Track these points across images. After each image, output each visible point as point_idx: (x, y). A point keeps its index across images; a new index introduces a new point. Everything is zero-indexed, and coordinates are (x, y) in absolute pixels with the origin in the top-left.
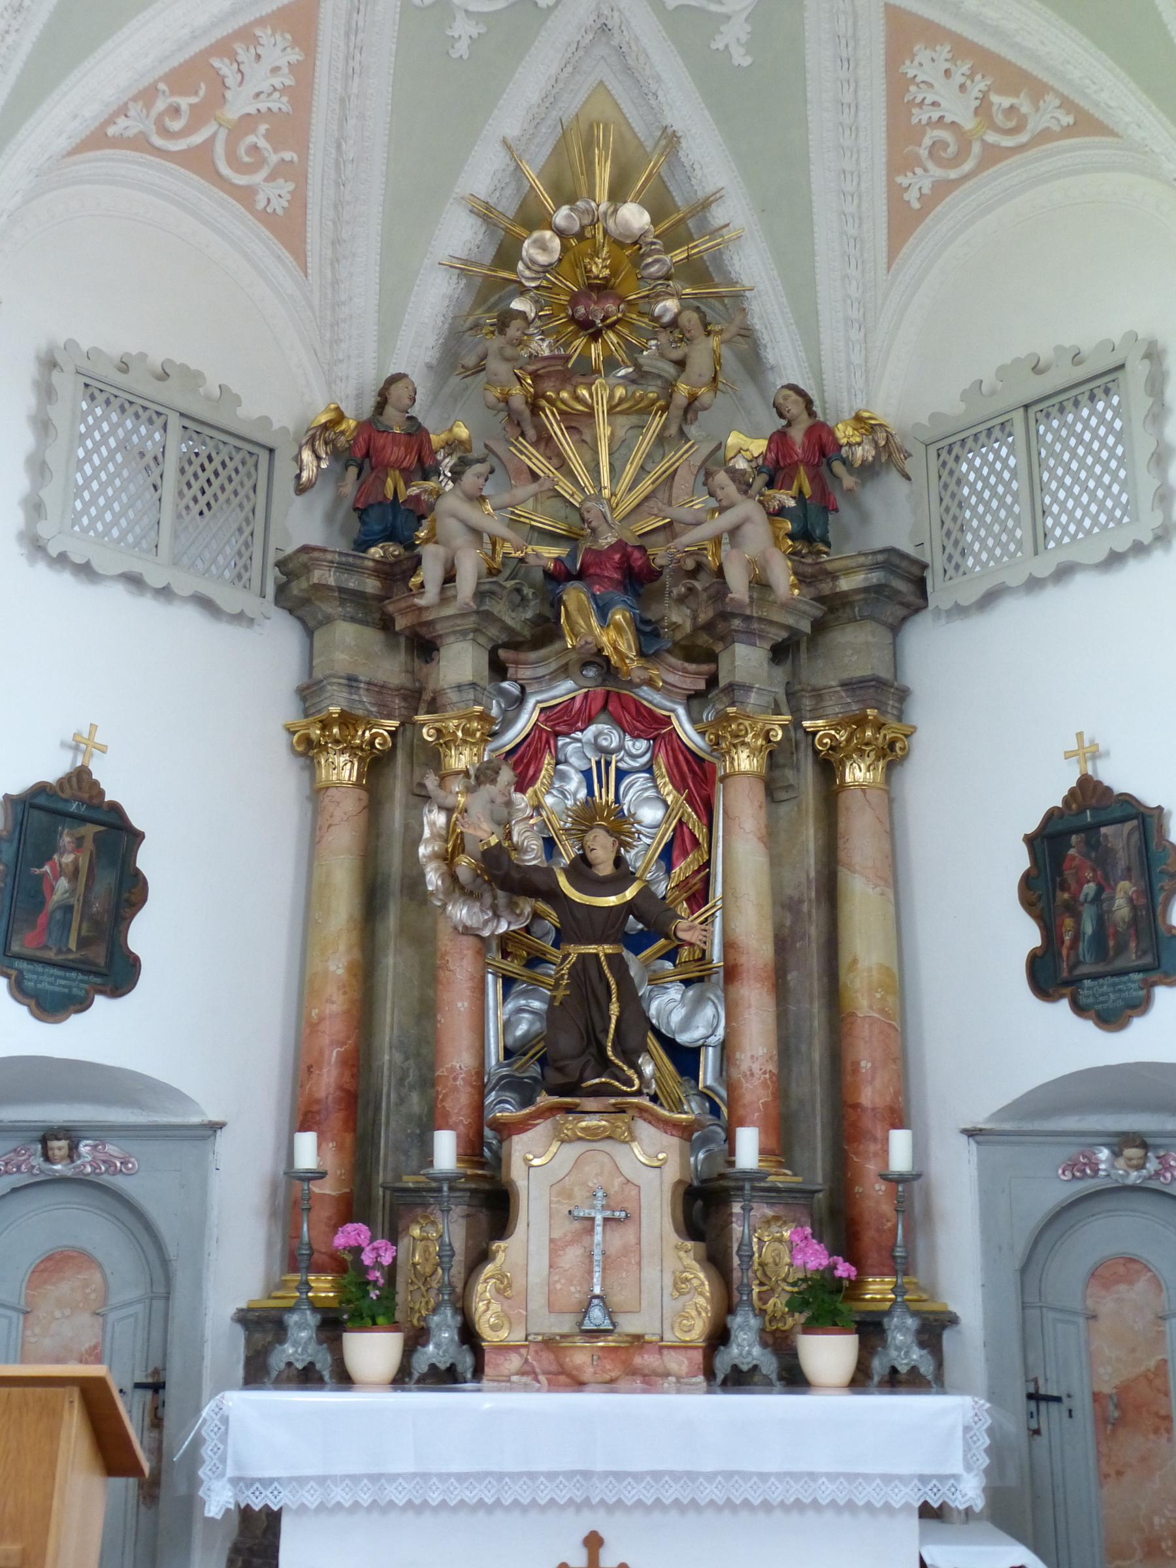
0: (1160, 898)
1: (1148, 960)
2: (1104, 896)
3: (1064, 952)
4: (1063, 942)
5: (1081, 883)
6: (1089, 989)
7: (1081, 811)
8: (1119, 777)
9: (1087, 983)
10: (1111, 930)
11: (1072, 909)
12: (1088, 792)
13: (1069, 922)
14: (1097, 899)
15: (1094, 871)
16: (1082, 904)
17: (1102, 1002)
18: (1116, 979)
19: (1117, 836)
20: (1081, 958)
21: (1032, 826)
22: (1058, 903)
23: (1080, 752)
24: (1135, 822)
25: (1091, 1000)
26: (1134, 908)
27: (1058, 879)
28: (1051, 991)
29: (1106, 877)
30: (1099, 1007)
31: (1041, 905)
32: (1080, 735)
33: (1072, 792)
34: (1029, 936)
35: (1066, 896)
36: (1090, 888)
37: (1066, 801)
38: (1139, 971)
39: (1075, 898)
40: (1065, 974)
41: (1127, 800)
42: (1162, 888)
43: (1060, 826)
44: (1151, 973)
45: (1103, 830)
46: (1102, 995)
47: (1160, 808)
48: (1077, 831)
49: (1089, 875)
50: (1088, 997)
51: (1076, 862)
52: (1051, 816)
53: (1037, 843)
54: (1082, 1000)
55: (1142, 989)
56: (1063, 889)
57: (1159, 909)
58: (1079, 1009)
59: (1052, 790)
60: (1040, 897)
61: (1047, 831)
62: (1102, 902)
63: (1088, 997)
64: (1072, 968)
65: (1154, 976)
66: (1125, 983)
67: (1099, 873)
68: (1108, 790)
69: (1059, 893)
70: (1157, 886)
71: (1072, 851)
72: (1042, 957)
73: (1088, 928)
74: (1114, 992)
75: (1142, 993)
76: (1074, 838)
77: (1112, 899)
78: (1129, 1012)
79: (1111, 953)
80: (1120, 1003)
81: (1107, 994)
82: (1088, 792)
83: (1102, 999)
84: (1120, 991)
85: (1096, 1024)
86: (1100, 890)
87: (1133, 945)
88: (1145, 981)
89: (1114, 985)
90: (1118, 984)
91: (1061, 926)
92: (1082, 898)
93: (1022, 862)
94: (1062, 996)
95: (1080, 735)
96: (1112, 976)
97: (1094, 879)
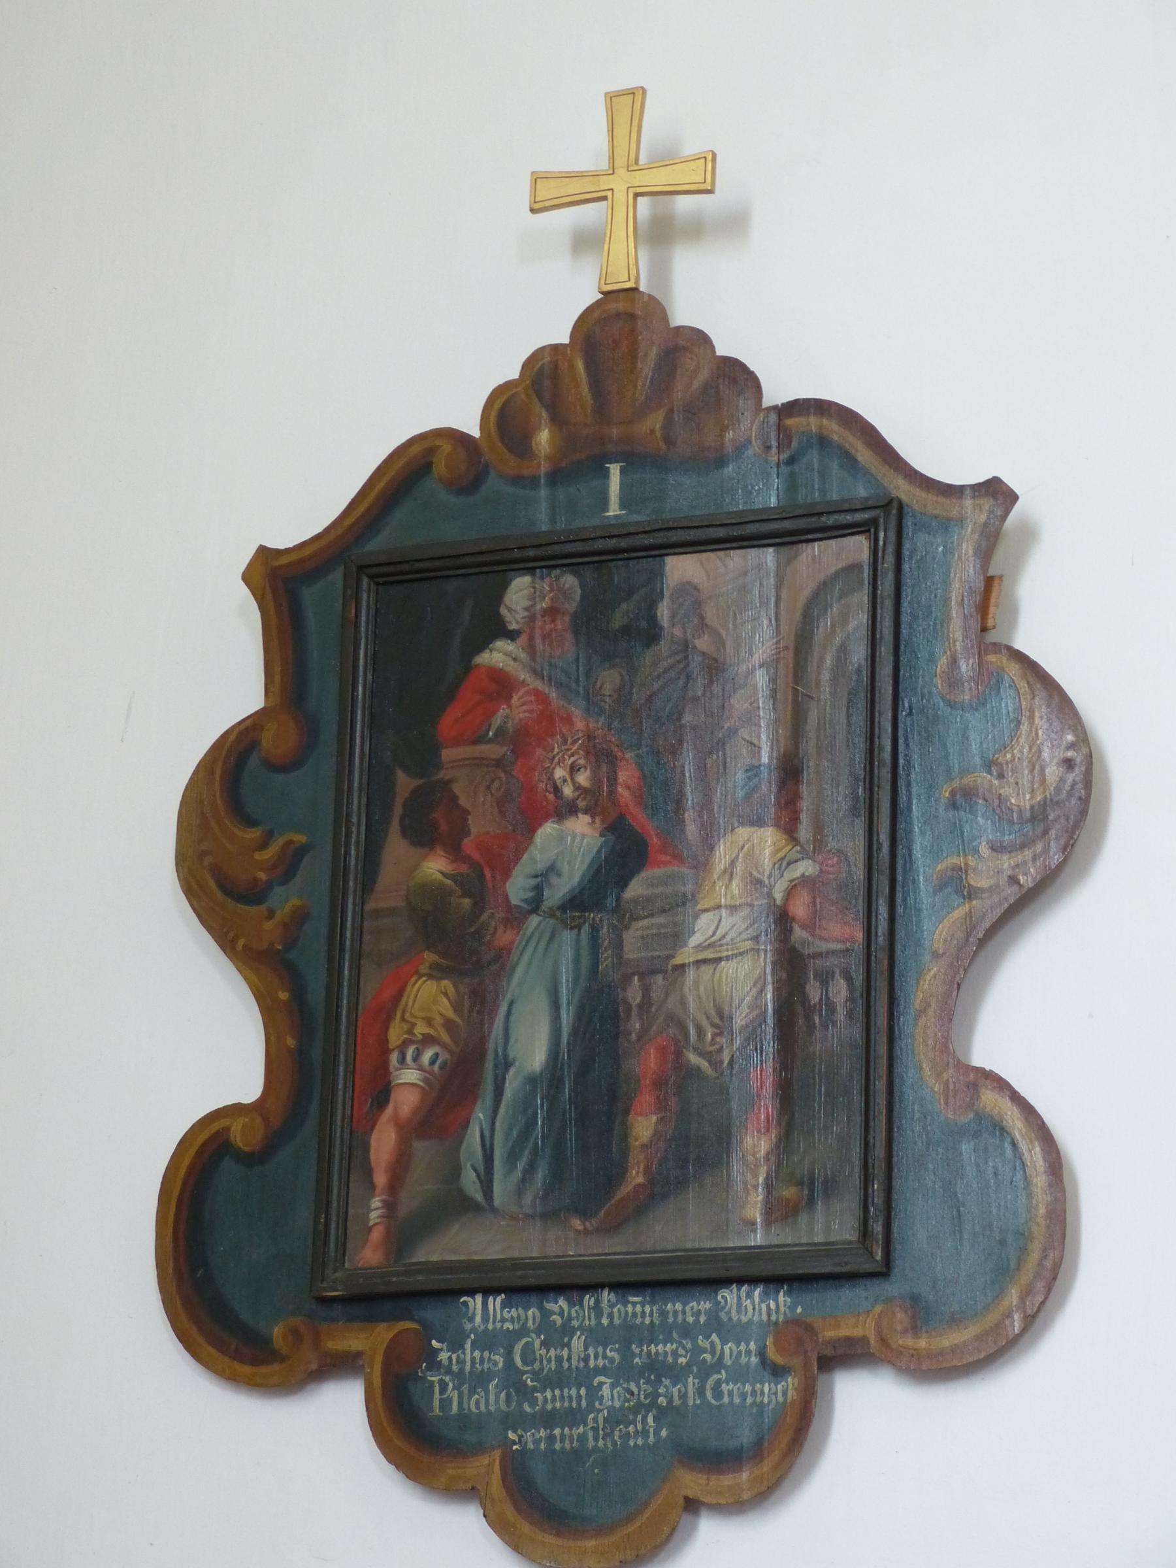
0: (937, 927)
1: (833, 1225)
2: (636, 889)
3: (383, 1143)
4: (382, 1094)
5: (534, 809)
6: (487, 1342)
7: (580, 465)
8: (783, 318)
9: (484, 1312)
10: (647, 1062)
11: (462, 940)
12: (624, 380)
13: (430, 998)
14: (597, 896)
15: (602, 756)
16: (514, 918)
17: (549, 1419)
18: (639, 1308)
19: (742, 610)
20: (470, 1182)
21: (308, 504)
22: (389, 892)
23: (620, 185)
24: (857, 547)
25: (492, 1400)
26: (792, 965)
27: (404, 783)
28: (278, 1333)
29: (662, 793)
30: (534, 1438)
31: (285, 901)
32: (626, 106)
33: (544, 370)
34: (207, 1044)
35: (435, 867)
36: (568, 845)
37: (504, 409)
38: (772, 1281)
39: (480, 878)
40: (369, 1254)
41: (827, 432)
42: (957, 884)
43: (450, 525)
44: (847, 1295)
45: (681, 569)
46: (558, 1379)
47: (997, 493)
48: (540, 557)
49: (569, 774)
50: (480, 1380)
51: (514, 712)
52: (411, 472)
53: (322, 599)
54: (444, 1397)
55: (777, 1372)
56: (423, 836)
57: (924, 984)
58: (416, 1438)
59: (442, 343)
60: (289, 865)
61: (379, 544)
62: (624, 915)
63: (480, 1380)
64: (404, 1234)
65: (849, 1313)
66: (686, 1331)
67: (626, 775)
68: (737, 377)
69: (396, 848)
70: (926, 863)
71: (499, 655)
72: (249, 1160)
73: (531, 1039)
74: (623, 1372)
75: (776, 1393)
76: (520, 595)
77: (678, 906)
78: (691, 1482)
79: (636, 1177)
80: (650, 1430)
81: (585, 1377)
82: (624, 380)
83: (548, 1399)
84: (657, 1369)
85: (499, 1525)
86: (626, 852)
87: (756, 1144)
88: (796, 1334)
89: (630, 1334)
90: (651, 1334)
91: (386, 1013)
92: (517, 888)
93: (224, 677)
94: (334, 1366)
95: (626, 106)
96: (623, 1287)
97: (595, 802)
